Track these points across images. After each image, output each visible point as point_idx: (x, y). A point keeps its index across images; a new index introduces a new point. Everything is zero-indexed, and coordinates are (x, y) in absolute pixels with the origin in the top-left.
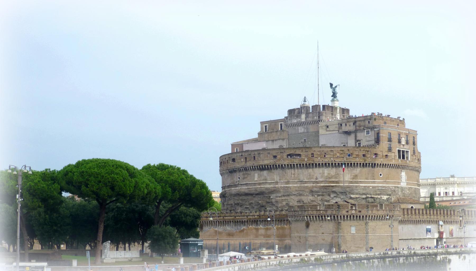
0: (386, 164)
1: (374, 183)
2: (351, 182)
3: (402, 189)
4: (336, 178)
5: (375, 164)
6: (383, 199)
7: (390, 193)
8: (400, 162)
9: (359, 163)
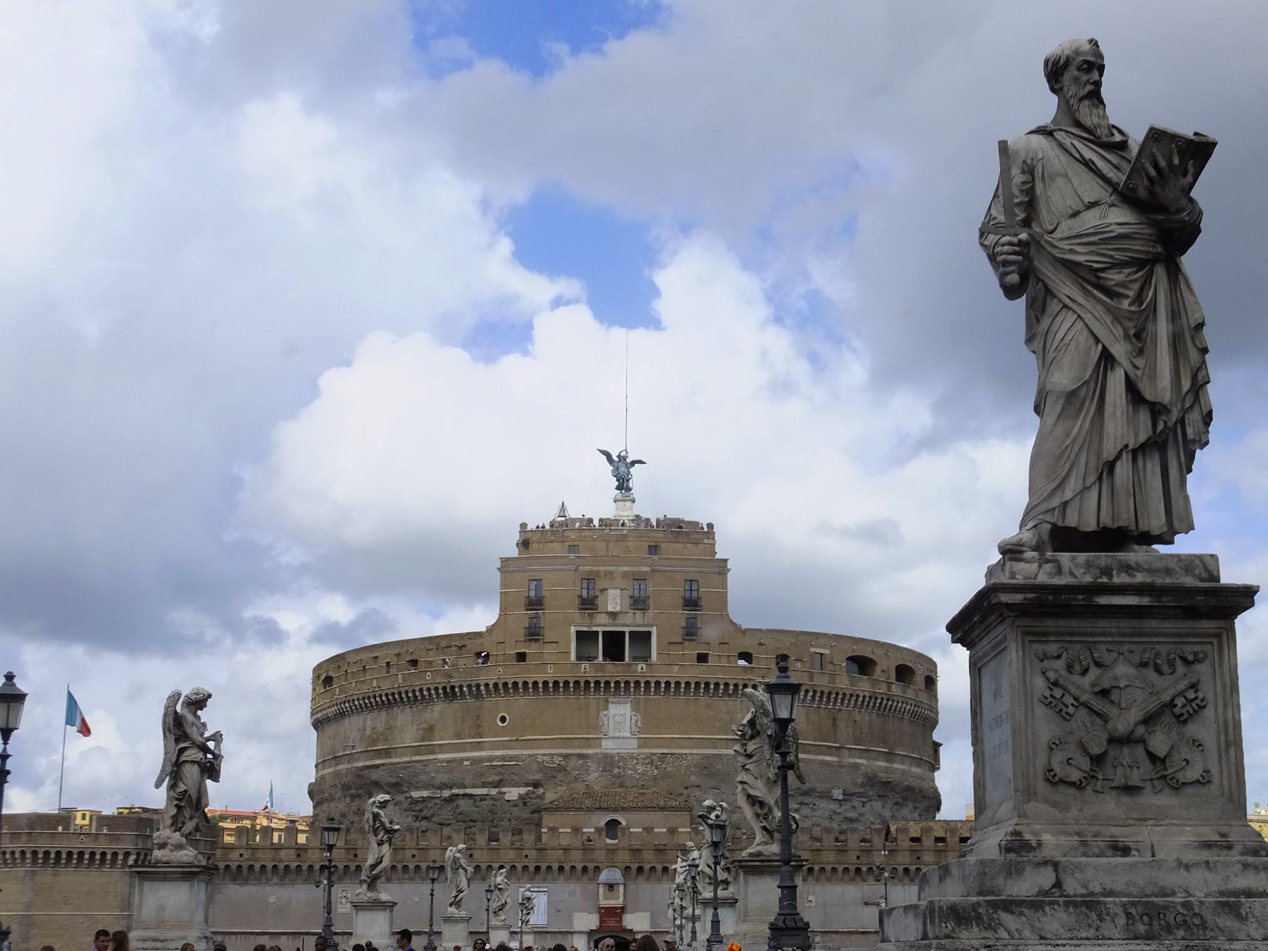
0: (515, 684)
1: (479, 746)
2: (417, 750)
3: (608, 762)
4: (386, 740)
5: (478, 686)
6: (507, 797)
7: (538, 776)
8: (598, 667)
9: (432, 687)
